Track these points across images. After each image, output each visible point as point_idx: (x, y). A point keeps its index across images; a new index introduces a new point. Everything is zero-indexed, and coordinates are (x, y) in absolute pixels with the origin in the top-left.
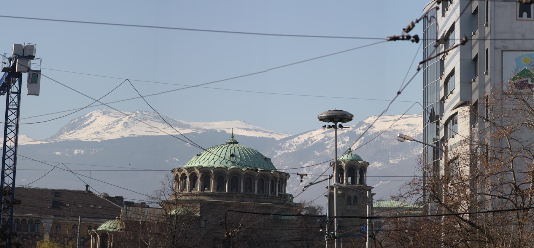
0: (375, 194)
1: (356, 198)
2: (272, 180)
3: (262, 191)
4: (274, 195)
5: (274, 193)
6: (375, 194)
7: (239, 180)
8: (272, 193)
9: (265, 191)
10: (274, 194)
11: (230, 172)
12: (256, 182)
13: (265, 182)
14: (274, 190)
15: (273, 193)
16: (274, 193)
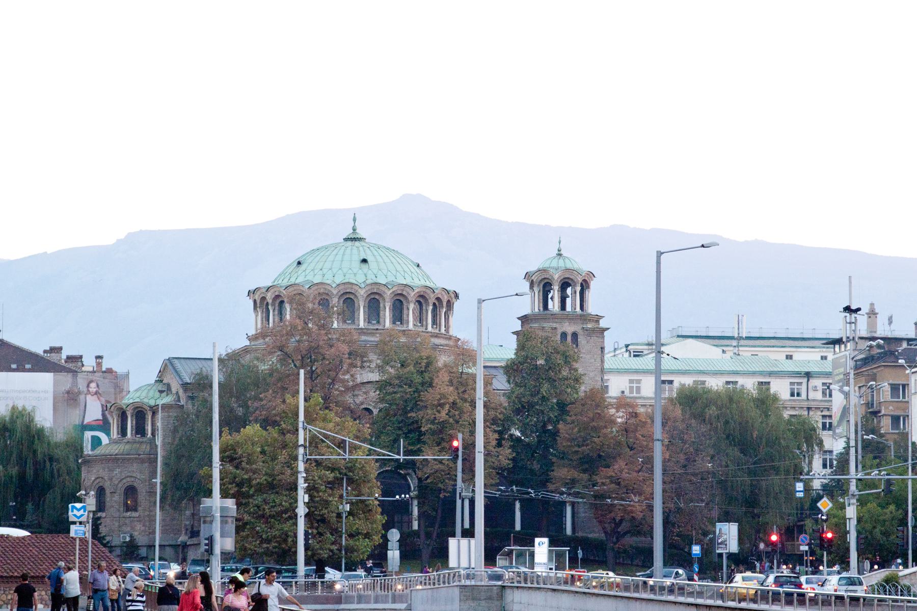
0: (609, 329)
1: (575, 335)
2: (434, 304)
3: (420, 323)
4: (437, 331)
5: (438, 327)
6: (609, 329)
7: (381, 305)
8: (435, 326)
9: (424, 323)
10: (438, 329)
11: (367, 291)
12: (412, 306)
13: (424, 308)
14: (438, 322)
15: (436, 328)
16: (438, 327)
